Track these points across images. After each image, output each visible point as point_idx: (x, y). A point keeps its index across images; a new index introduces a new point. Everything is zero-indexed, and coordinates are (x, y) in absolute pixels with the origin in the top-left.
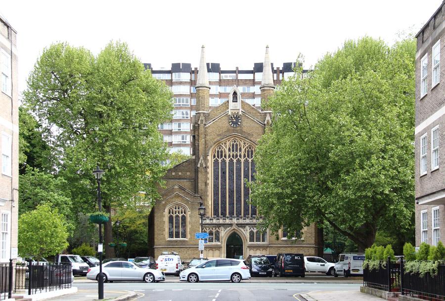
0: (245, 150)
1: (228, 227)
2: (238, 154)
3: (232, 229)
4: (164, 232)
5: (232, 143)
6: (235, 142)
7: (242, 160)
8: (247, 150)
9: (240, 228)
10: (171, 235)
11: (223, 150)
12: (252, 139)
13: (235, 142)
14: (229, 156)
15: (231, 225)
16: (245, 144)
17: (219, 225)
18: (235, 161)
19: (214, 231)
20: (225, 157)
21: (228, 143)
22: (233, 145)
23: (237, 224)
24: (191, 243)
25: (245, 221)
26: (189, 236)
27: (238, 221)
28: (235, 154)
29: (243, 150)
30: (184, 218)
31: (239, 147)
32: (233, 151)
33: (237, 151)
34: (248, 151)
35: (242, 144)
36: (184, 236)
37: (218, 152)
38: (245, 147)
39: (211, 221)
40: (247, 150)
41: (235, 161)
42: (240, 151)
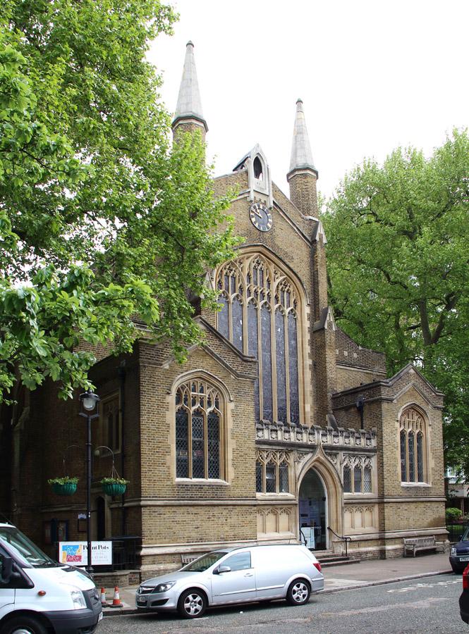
0: (278, 287)
1: (307, 453)
3: (315, 458)
4: (168, 457)
8: (280, 288)
10: (182, 472)
15: (313, 448)
17: (290, 447)
18: (260, 304)
21: (246, 263)
23: (325, 448)
24: (237, 492)
25: (336, 440)
26: (231, 473)
29: (274, 285)
30: (215, 421)
38: (278, 281)
40: (280, 288)
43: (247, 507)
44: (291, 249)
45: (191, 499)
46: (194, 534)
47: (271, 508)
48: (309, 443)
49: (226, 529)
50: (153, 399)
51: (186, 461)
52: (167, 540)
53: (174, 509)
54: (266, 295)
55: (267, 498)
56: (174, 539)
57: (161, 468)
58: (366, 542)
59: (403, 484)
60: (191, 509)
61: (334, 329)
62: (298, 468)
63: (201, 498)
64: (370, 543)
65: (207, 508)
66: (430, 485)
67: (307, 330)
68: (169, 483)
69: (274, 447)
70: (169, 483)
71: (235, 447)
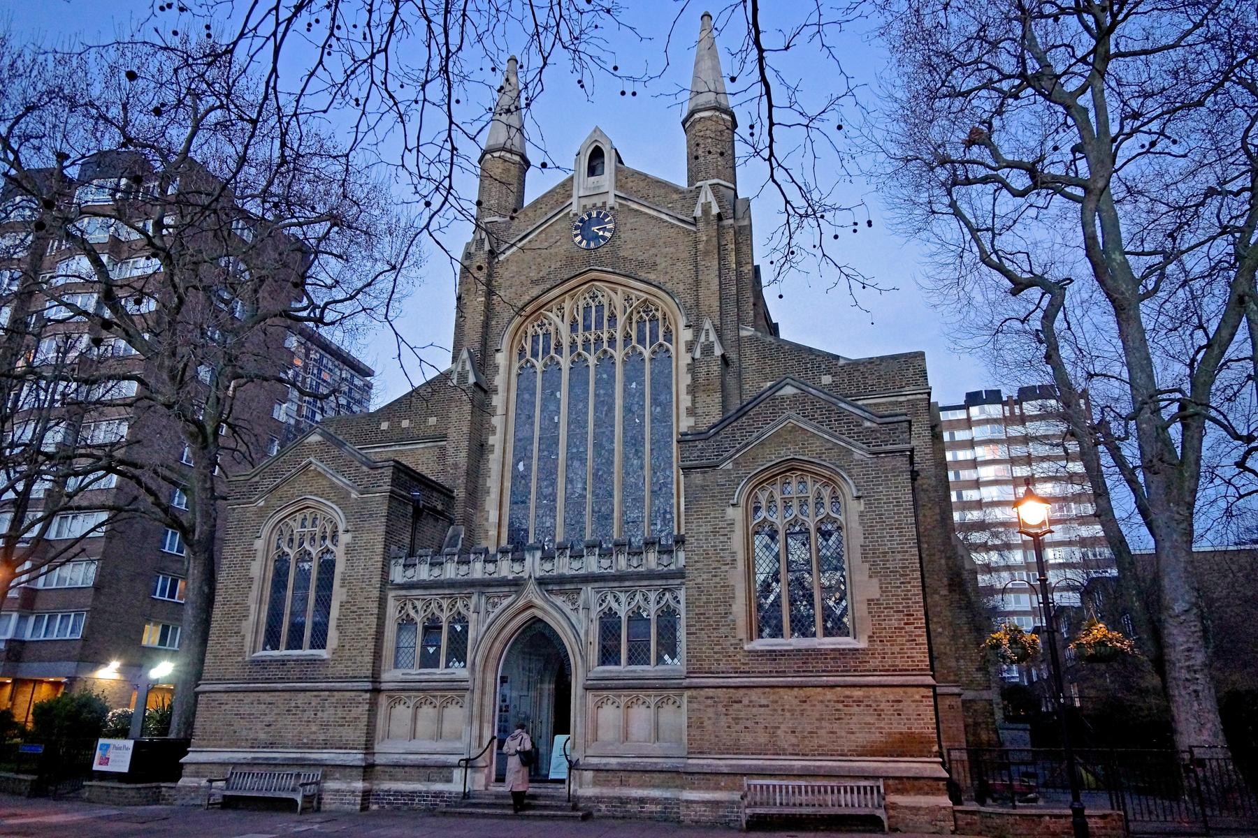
2: (605, 337)
3: (521, 603)
5: (581, 304)
6: (594, 298)
7: (619, 354)
9: (558, 600)
11: (552, 329)
12: (652, 277)
13: (594, 298)
14: (573, 345)
15: (517, 584)
16: (628, 299)
18: (592, 361)
19: (444, 617)
20: (559, 348)
22: (587, 309)
23: (542, 582)
24: (340, 669)
27: (548, 566)
28: (592, 338)
29: (621, 320)
31: (606, 314)
32: (587, 328)
33: (599, 325)
34: (641, 322)
35: (618, 300)
36: (319, 640)
37: (535, 337)
38: (629, 310)
39: (436, 572)
40: (635, 318)
41: (592, 361)
42: (612, 318)
43: (353, 694)
44: (653, 251)
45: (268, 680)
46: (262, 736)
47: (421, 694)
48: (510, 577)
49: (314, 729)
50: (238, 549)
51: (302, 625)
52: (223, 743)
53: (241, 696)
54: (605, 340)
55: (401, 677)
56: (234, 743)
57: (233, 639)
58: (647, 777)
59: (764, 644)
60: (264, 696)
61: (718, 351)
62: (487, 624)
63: (282, 680)
64: (658, 778)
65: (287, 695)
66: (862, 644)
67: (685, 369)
68: (240, 659)
69: (434, 592)
70: (240, 659)
71: (344, 598)
